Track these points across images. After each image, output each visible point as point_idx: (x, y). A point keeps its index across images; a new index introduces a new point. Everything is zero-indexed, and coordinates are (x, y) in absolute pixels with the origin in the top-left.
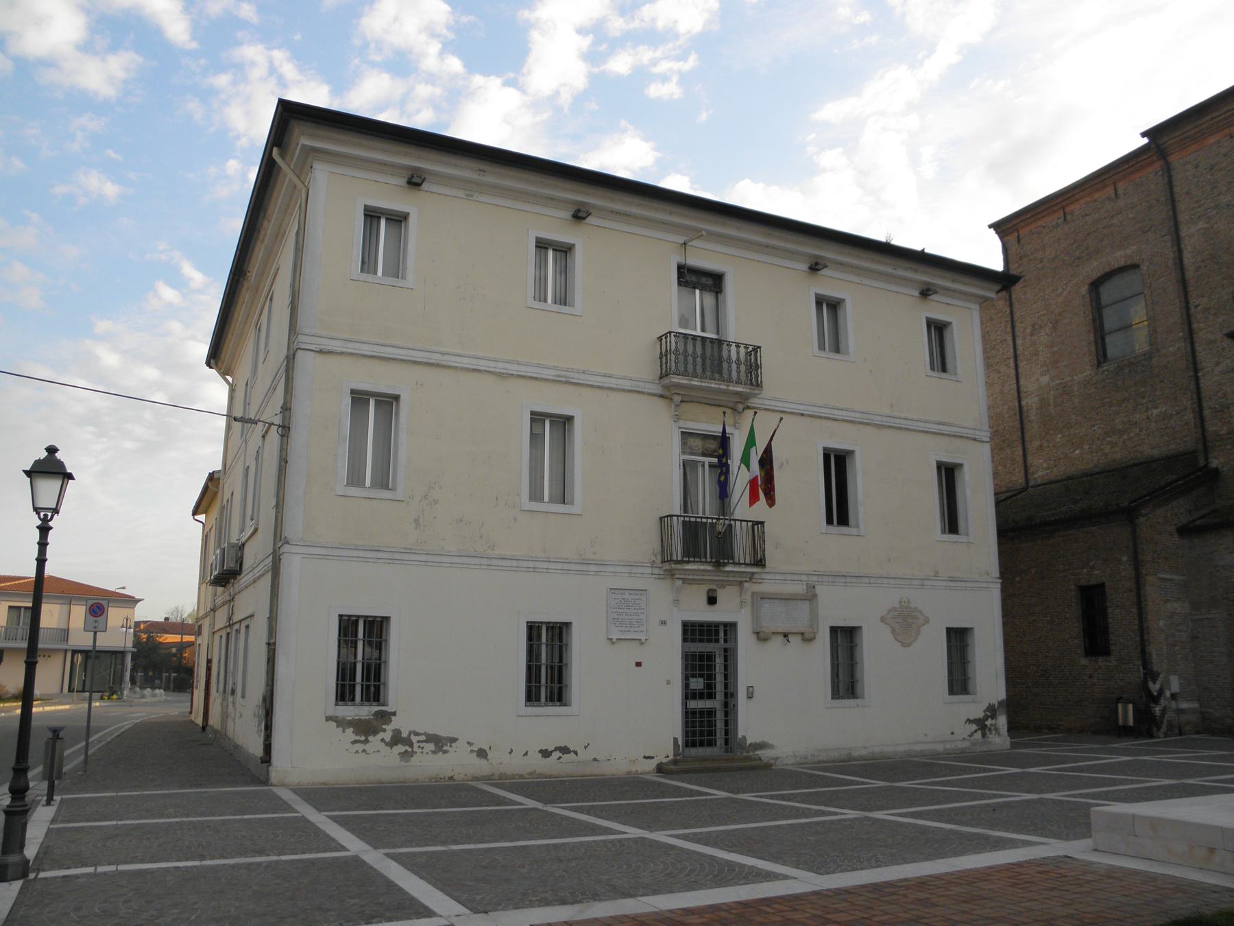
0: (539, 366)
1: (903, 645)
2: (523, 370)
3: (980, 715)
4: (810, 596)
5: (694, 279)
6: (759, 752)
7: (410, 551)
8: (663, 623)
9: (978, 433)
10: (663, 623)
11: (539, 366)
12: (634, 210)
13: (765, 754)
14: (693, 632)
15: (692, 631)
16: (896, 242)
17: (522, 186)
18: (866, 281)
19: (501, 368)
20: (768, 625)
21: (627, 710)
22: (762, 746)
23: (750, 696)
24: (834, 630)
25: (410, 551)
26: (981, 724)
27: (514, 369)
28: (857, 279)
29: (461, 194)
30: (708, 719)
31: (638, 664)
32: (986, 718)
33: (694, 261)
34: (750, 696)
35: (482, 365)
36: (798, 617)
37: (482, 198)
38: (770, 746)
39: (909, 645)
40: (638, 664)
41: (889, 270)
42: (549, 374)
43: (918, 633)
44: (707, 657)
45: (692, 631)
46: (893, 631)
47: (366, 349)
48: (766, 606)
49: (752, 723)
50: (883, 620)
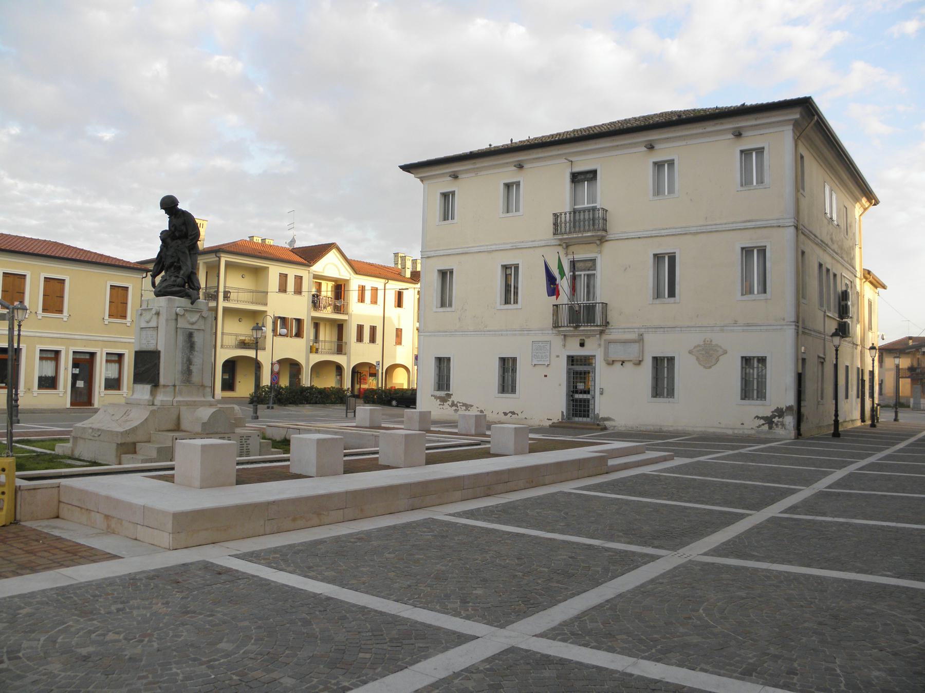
0: (504, 244)
1: (705, 367)
2: (498, 247)
3: (769, 414)
4: (640, 340)
5: (583, 177)
6: (606, 423)
7: (456, 331)
8: (558, 356)
9: (781, 221)
10: (558, 356)
11: (504, 244)
12: (540, 155)
13: (607, 423)
14: (573, 361)
15: (572, 360)
16: (749, 103)
17: (491, 163)
18: (690, 142)
19: (489, 248)
20: (612, 357)
21: (543, 396)
22: (608, 419)
23: (602, 394)
24: (655, 359)
25: (456, 331)
26: (769, 421)
27: (494, 247)
28: (684, 143)
29: (473, 174)
30: (579, 405)
31: (546, 376)
32: (774, 416)
33: (578, 169)
34: (602, 394)
35: (482, 249)
36: (633, 351)
37: (482, 173)
38: (613, 420)
39: (710, 367)
40: (546, 376)
41: (700, 131)
42: (508, 246)
43: (717, 360)
44: (579, 372)
45: (572, 360)
46: (698, 359)
47: (442, 253)
48: (612, 346)
49: (602, 407)
50: (690, 352)
